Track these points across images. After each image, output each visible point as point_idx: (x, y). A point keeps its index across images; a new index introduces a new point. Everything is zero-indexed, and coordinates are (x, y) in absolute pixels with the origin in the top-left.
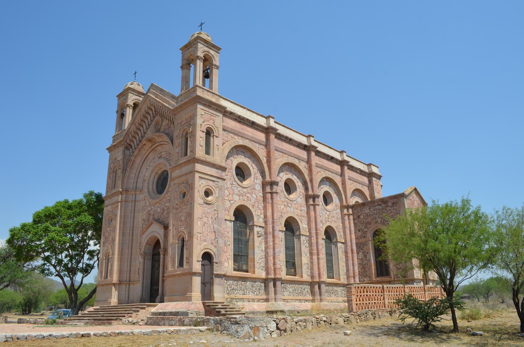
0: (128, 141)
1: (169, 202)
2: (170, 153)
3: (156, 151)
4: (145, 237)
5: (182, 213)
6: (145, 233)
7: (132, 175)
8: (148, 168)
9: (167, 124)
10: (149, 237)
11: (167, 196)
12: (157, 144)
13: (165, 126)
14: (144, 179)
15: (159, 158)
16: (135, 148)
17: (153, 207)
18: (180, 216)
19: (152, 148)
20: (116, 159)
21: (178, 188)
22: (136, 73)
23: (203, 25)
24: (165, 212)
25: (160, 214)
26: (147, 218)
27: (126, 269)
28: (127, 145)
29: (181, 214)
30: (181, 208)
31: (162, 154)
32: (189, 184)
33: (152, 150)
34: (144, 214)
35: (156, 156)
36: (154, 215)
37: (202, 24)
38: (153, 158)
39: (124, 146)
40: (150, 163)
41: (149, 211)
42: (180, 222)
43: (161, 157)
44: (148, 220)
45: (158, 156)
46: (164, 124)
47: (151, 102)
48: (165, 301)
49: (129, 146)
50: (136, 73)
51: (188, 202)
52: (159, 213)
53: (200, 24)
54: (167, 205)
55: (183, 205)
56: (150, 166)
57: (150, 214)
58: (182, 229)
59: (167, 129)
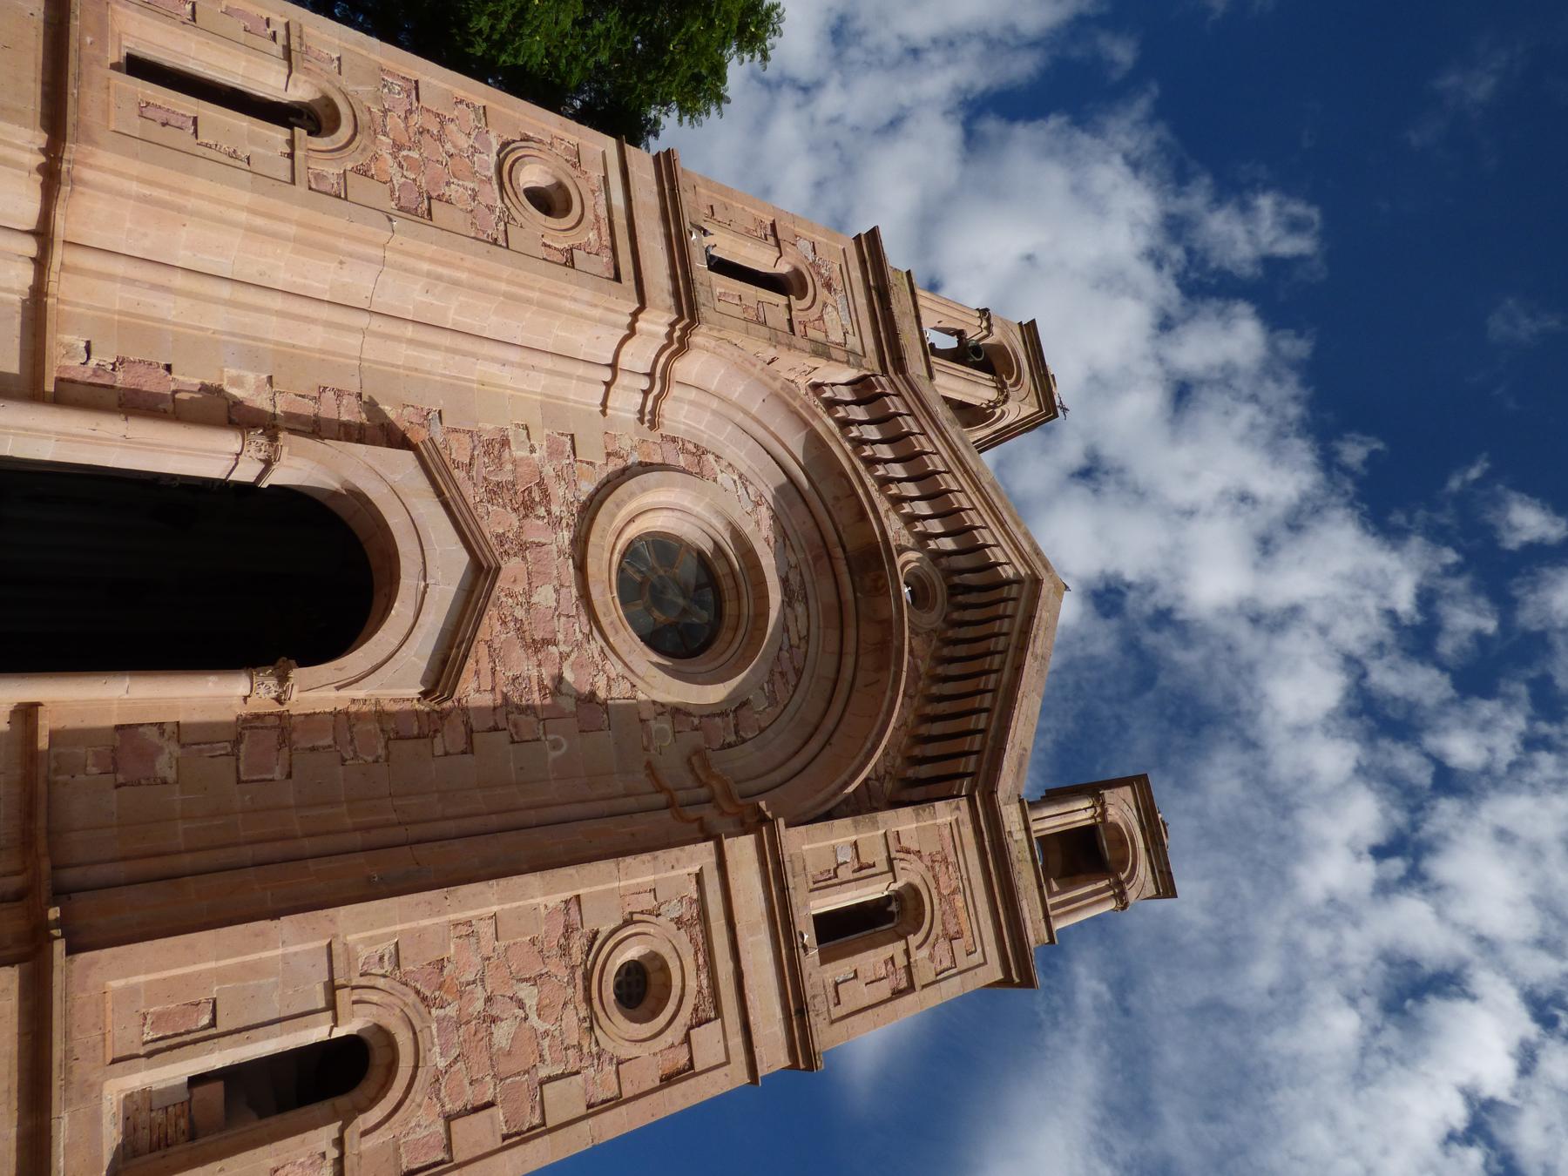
0: (894, 405)
2: (799, 673)
3: (816, 559)
4: (395, 478)
6: (422, 482)
7: (740, 389)
10: (396, 521)
11: (613, 675)
12: (848, 594)
15: (785, 581)
16: (845, 424)
17: (566, 536)
18: (528, 994)
19: (838, 552)
20: (828, 286)
21: (679, 922)
26: (505, 476)
27: (183, 258)
28: (879, 390)
30: (570, 991)
31: (800, 608)
33: (822, 537)
34: (533, 450)
35: (793, 561)
36: (524, 547)
38: (790, 532)
39: (877, 370)
41: (546, 494)
42: (479, 1005)
44: (495, 491)
45: (791, 576)
49: (866, 394)
52: (528, 594)
57: (528, 507)
58: (437, 1049)
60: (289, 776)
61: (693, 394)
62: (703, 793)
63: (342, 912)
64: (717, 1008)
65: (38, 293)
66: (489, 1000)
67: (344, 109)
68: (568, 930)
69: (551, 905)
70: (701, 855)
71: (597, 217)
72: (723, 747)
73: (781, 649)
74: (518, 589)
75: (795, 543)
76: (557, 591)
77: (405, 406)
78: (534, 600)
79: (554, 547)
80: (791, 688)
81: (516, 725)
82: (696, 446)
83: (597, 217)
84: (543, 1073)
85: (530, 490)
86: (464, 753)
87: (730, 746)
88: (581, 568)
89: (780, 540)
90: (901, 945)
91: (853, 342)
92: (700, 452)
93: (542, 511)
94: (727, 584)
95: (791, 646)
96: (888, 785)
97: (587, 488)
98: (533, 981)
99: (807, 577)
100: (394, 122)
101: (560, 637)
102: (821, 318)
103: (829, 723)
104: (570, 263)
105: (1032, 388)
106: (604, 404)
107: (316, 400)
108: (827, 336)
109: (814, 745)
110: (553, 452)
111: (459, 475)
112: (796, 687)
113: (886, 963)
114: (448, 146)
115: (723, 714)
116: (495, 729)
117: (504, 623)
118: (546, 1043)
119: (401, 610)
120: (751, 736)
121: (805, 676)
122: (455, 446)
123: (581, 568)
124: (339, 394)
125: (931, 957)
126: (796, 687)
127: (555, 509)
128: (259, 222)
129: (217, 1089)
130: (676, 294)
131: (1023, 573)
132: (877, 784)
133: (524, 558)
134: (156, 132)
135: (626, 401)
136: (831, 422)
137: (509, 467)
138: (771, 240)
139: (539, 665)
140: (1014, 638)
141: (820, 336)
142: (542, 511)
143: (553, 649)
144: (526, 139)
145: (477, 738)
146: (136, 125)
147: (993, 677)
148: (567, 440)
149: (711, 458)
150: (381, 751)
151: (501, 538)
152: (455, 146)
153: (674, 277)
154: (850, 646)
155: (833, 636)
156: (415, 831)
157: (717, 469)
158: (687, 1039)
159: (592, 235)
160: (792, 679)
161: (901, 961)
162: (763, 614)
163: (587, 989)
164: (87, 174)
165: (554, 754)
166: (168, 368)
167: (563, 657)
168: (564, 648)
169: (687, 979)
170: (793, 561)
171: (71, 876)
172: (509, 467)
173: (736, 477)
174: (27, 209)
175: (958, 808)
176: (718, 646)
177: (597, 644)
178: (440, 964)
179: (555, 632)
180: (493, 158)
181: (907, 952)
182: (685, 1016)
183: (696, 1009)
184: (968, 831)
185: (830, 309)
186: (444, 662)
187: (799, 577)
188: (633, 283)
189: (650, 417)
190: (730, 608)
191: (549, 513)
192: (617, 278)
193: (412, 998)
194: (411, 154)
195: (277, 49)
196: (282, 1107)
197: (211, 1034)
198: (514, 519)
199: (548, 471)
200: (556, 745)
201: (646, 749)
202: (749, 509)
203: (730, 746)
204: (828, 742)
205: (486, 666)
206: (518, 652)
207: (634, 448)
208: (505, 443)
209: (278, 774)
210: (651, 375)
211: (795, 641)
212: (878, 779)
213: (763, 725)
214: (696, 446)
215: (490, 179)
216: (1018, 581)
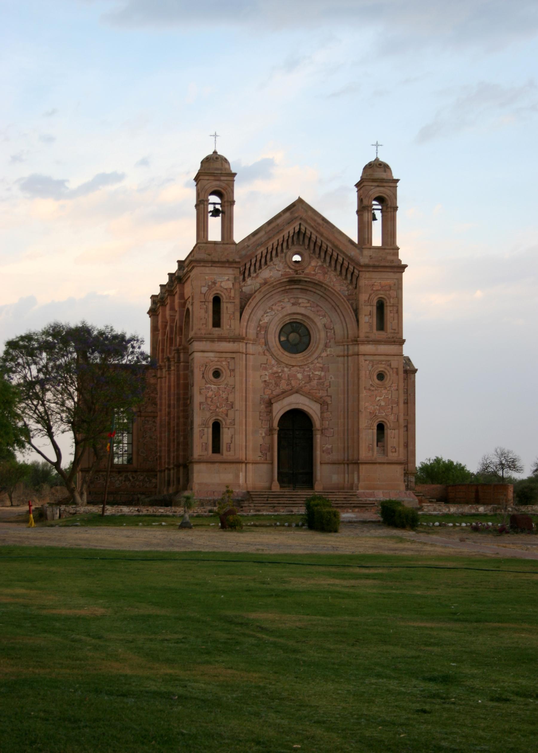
1: (322, 371)
2: (317, 305)
5: (380, 397)
8: (269, 311)
9: (320, 266)
12: (300, 287)
13: (316, 267)
14: (259, 324)
15: (293, 304)
17: (286, 369)
18: (378, 398)
19: (288, 287)
20: (214, 283)
21: (373, 366)
22: (215, 136)
23: (379, 148)
24: (315, 382)
25: (303, 382)
26: (273, 382)
29: (378, 398)
30: (379, 391)
32: (392, 367)
34: (266, 375)
36: (289, 379)
37: (377, 145)
38: (279, 300)
40: (273, 305)
41: (277, 372)
42: (378, 407)
43: (299, 304)
44: (277, 385)
46: (313, 264)
47: (303, 228)
48: (359, 488)
50: (215, 136)
51: (390, 387)
52: (299, 380)
53: (375, 143)
54: (317, 373)
55: (383, 389)
56: (272, 309)
57: (279, 377)
59: (320, 273)
60: (333, 429)
61: (248, 330)
62: (346, 347)
63: (360, 427)
64: (389, 361)
65: (253, 463)
66: (377, 405)
67: (214, 418)
68: (370, 390)
69: (365, 392)
70: (362, 358)
71: (218, 361)
72: (335, 334)
73: (311, 310)
74: (298, 382)
75: (283, 298)
76: (298, 373)
77: (260, 403)
78: (300, 379)
79: (289, 372)
80: (321, 309)
81: (327, 386)
82: (258, 327)
83: (218, 361)
84: (390, 397)
85: (276, 377)
86: (331, 397)
87: (334, 332)
88: (293, 366)
89: (282, 303)
90: (388, 308)
91: (231, 277)
92: (259, 326)
93: (280, 374)
94: (292, 321)
95: (310, 306)
96: (350, 287)
97: (273, 362)
98: (376, 397)
99: (292, 296)
100: (212, 407)
101: (309, 373)
102: (226, 289)
103: (334, 304)
104: (233, 370)
105: (226, 182)
106: (253, 355)
107: (262, 420)
108: (231, 289)
109: (338, 311)
110: (265, 369)
111: (274, 393)
112: (321, 308)
113: (391, 313)
114: (213, 396)
115: (327, 331)
116: (327, 390)
117: (306, 386)
118: (386, 396)
119: (305, 408)
120: (332, 325)
121: (318, 304)
122: (268, 393)
123: (293, 366)
124: (260, 416)
125: (393, 298)
126: (321, 308)
127: (280, 371)
128: (241, 433)
129: (379, 443)
130: (234, 342)
131: (298, 223)
132: (349, 291)
133: (291, 380)
134: (232, 449)
135: (251, 348)
136: (249, 281)
137: (271, 381)
138: (206, 303)
139: (314, 379)
140: (319, 236)
141: (232, 291)
142: (280, 374)
143: (311, 375)
144: (203, 377)
145: (329, 395)
146: (232, 453)
147: (329, 249)
148: (262, 365)
149: (261, 323)
150: (329, 413)
151: (288, 385)
152: (212, 395)
153: (229, 341)
154: (314, 290)
155: (308, 292)
156: (346, 410)
157: (264, 321)
158: (392, 369)
159: (224, 363)
160: (319, 308)
161: (391, 308)
162: (302, 315)
163: (380, 387)
164: (241, 458)
165: (333, 379)
166: (261, 445)
167: (313, 373)
168: (311, 373)
169: (381, 368)
170: (286, 300)
171: (346, 459)
172: (271, 381)
173: (265, 315)
174: (244, 465)
175: (361, 277)
176: (310, 330)
177: (311, 366)
178: (370, 413)
179: (308, 375)
180: (213, 386)
181: (390, 306)
182: (388, 368)
183: (388, 366)
184: (368, 275)
185: (222, 285)
186: (315, 401)
187: (292, 299)
188: (234, 354)
189: (255, 342)
190: (298, 321)
191: (280, 372)
192: (234, 358)
193: (374, 418)
194: (218, 405)
195: (206, 429)
196: (383, 433)
197: (373, 445)
198: (283, 381)
199: (270, 371)
200: (331, 378)
201: (333, 356)
202: (274, 313)
203: (334, 332)
204: (338, 306)
205: (314, 391)
206: (312, 383)
207: (262, 347)
208: (265, 381)
209: (332, 430)
210: (246, 343)
211: (309, 305)
212: (348, 291)
213: (330, 321)
214: (258, 327)
215: (218, 388)
216: (300, 224)
